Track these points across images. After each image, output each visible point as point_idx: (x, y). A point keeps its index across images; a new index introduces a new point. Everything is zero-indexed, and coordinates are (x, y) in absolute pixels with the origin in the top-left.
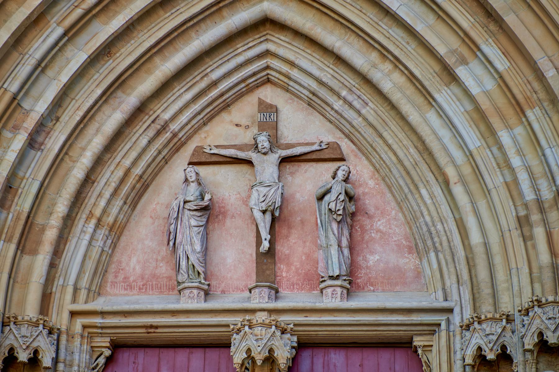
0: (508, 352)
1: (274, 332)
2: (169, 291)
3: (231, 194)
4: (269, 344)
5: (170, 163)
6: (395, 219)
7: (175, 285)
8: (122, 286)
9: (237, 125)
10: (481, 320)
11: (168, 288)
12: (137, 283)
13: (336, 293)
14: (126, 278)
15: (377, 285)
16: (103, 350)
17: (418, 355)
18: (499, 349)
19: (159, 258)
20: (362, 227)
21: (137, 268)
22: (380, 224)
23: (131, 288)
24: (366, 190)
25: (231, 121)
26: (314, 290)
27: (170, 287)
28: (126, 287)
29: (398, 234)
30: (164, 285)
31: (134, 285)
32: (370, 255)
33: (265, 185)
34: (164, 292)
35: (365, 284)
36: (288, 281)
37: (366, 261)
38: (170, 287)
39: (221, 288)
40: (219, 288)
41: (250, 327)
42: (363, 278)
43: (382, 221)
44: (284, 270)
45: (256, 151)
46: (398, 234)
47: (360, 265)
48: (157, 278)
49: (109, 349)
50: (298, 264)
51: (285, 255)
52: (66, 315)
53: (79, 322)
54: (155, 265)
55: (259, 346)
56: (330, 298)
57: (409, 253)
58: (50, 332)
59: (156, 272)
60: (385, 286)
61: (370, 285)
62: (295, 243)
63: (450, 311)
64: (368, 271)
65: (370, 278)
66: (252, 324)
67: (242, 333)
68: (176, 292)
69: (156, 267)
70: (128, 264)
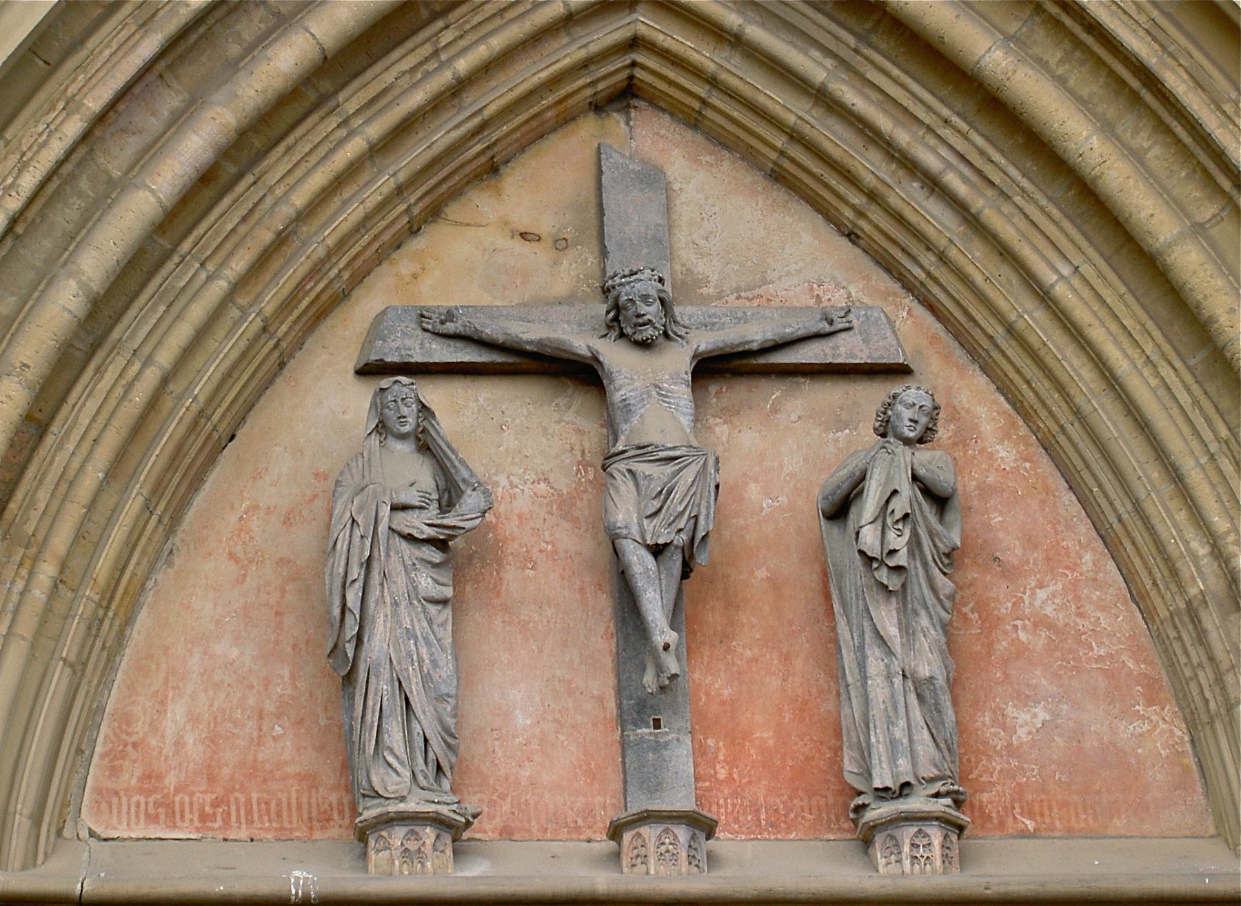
2: (311, 828)
3: (515, 480)
5: (292, 364)
6: (1094, 580)
7: (330, 805)
8: (138, 805)
9: (523, 235)
11: (305, 816)
12: (192, 795)
13: (925, 841)
14: (151, 778)
15: (1046, 812)
19: (270, 707)
20: (983, 607)
21: (190, 739)
23: (171, 814)
25: (505, 223)
26: (830, 830)
27: (314, 814)
28: (151, 811)
29: (1109, 636)
30: (289, 804)
31: (182, 804)
32: (1015, 706)
33: (662, 454)
34: (291, 830)
35: (1005, 808)
36: (735, 794)
38: (314, 814)
39: (498, 820)
40: (491, 817)
42: (999, 788)
43: (1051, 589)
44: (721, 757)
45: (614, 334)
46: (1109, 636)
47: (986, 743)
48: (265, 781)
50: (766, 736)
51: (723, 703)
57: (1150, 702)
59: (260, 756)
60: (1073, 818)
64: (1014, 763)
65: (1020, 788)
68: (338, 830)
69: (260, 737)
70: (154, 728)
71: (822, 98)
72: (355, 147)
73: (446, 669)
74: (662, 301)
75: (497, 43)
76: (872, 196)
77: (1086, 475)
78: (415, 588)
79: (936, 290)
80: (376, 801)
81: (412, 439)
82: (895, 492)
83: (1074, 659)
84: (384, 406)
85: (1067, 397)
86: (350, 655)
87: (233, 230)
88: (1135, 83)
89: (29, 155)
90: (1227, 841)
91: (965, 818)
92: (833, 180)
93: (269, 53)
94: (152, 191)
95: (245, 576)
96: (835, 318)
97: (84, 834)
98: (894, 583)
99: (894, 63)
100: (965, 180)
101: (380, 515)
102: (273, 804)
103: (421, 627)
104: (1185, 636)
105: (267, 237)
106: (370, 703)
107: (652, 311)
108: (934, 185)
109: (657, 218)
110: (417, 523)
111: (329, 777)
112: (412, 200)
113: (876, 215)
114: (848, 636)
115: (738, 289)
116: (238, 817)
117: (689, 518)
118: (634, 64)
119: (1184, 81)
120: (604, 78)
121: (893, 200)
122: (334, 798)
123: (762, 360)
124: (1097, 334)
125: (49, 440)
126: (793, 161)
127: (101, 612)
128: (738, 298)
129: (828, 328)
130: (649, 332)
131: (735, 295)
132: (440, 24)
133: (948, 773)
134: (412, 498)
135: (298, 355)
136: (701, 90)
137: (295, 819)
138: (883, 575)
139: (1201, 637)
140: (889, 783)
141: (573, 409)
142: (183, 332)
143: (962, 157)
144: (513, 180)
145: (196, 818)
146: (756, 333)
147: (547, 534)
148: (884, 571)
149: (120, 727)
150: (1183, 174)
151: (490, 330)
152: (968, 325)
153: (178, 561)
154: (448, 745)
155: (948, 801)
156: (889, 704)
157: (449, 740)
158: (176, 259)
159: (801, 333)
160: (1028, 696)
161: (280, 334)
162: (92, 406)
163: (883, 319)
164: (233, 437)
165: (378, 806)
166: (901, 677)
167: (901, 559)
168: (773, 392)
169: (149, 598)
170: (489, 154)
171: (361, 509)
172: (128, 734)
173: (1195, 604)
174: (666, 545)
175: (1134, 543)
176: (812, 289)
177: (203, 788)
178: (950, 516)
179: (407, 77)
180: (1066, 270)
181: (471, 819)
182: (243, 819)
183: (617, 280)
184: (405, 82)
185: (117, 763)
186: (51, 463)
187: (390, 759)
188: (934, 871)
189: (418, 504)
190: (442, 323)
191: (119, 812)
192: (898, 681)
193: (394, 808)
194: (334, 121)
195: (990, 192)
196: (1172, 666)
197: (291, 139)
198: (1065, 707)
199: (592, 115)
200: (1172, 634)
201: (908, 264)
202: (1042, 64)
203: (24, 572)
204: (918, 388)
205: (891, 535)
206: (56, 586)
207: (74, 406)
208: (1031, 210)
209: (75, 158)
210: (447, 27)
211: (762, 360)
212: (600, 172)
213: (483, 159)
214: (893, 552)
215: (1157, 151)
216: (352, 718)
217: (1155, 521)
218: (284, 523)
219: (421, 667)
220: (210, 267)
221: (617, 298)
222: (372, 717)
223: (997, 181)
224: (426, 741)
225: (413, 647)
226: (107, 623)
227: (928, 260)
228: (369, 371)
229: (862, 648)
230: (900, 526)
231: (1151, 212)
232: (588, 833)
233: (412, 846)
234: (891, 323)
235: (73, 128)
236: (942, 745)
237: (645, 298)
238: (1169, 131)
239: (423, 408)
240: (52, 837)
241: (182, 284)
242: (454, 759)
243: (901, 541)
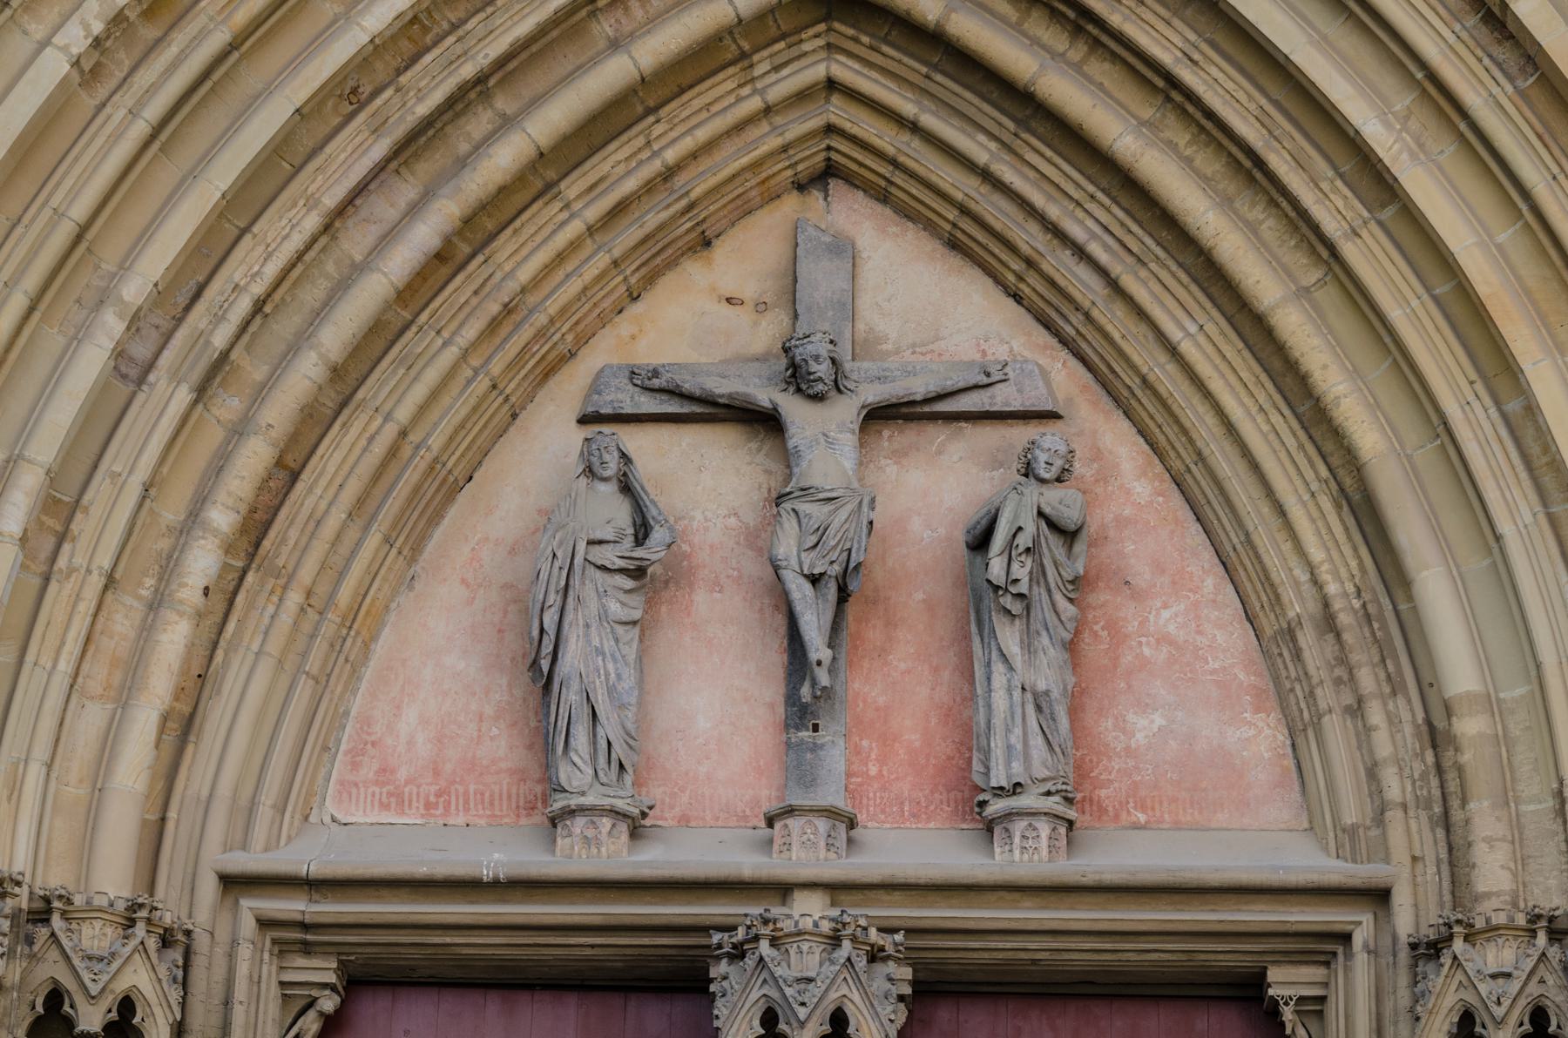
0: (1552, 1029)
1: (849, 959)
2: (518, 816)
4: (833, 995)
5: (523, 415)
6: (1214, 601)
8: (373, 796)
9: (728, 300)
10: (1473, 930)
11: (514, 806)
13: (1035, 834)
15: (1157, 806)
16: (315, 993)
17: (1282, 1025)
18: (1526, 1020)
19: (489, 711)
20: (1112, 626)
22: (1168, 617)
24: (1127, 512)
26: (964, 820)
27: (521, 803)
28: (384, 799)
30: (501, 795)
31: (410, 794)
32: (1135, 713)
33: (821, 496)
35: (1121, 803)
36: (883, 789)
37: (1124, 731)
39: (677, 809)
40: (672, 807)
41: (774, 942)
42: (1116, 785)
43: (1174, 609)
44: (873, 756)
48: (481, 774)
49: (333, 988)
50: (915, 738)
51: (877, 709)
52: (208, 887)
53: (252, 905)
54: (475, 734)
55: (803, 1004)
56: (1017, 852)
57: (1257, 710)
58: (166, 941)
61: (1135, 808)
62: (909, 672)
63: (1379, 897)
64: (1131, 763)
66: (780, 934)
67: (750, 962)
68: (539, 818)
69: (479, 737)
71: (986, 175)
72: (576, 228)
73: (628, 682)
74: (833, 361)
75: (702, 135)
76: (1030, 263)
77: (1206, 507)
78: (606, 611)
79: (1084, 345)
80: (563, 795)
81: (615, 481)
82: (1020, 529)
83: (1191, 671)
84: (590, 454)
85: (1191, 441)
86: (545, 669)
87: (466, 302)
88: (1248, 164)
89: (273, 246)
91: (1072, 814)
92: (997, 249)
93: (491, 151)
94: (385, 274)
95: (474, 598)
96: (992, 370)
97: (327, 819)
98: (1016, 607)
99: (1049, 146)
100: (1106, 247)
101: (577, 548)
102: (487, 795)
103: (609, 645)
104: (1286, 653)
105: (494, 308)
106: (561, 710)
107: (822, 369)
108: (1081, 253)
109: (847, 286)
110: (608, 556)
111: (536, 773)
112: (628, 272)
113: (1033, 278)
114: (981, 653)
115: (914, 345)
116: (457, 805)
117: (842, 551)
118: (829, 148)
119: (1286, 162)
120: (802, 160)
121: (1045, 267)
122: (539, 789)
123: (927, 409)
124: (1216, 385)
125: (300, 487)
126: (963, 231)
127: (344, 631)
128: (914, 353)
129: (986, 380)
130: (820, 387)
131: (911, 350)
132: (651, 119)
133: (1062, 773)
134: (608, 534)
135: (530, 407)
136: (884, 170)
137: (505, 808)
138: (1007, 601)
139: (1297, 655)
140: (1004, 783)
141: (763, 452)
142: (419, 392)
143: (1106, 229)
144: (722, 251)
145: (421, 807)
146: (919, 387)
147: (734, 564)
148: (1009, 597)
149: (361, 728)
150: (1293, 243)
151: (687, 387)
152: (1111, 376)
153: (418, 585)
154: (631, 747)
155: (1057, 798)
156: (1008, 714)
157: (631, 742)
158: (414, 329)
159: (961, 385)
160: (1147, 705)
161: (508, 391)
162: (338, 457)
163: (1037, 371)
164: (471, 478)
165: (564, 799)
166: (1020, 690)
167: (1023, 588)
168: (938, 434)
169: (392, 617)
170: (700, 229)
171: (561, 544)
172: (369, 734)
173: (1293, 624)
174: (821, 575)
175: (1246, 570)
176: (978, 345)
177: (430, 780)
178: (1079, 547)
179: (622, 166)
180: (1193, 329)
181: (647, 811)
182: (461, 808)
183: (793, 342)
184: (621, 169)
185: (358, 759)
186: (302, 505)
187: (576, 759)
188: (1040, 861)
189: (612, 539)
190: (649, 379)
191: (357, 801)
192: (1017, 694)
193: (574, 802)
194: (557, 205)
195: (1130, 260)
196: (1276, 680)
197: (517, 223)
198: (1180, 714)
199: (795, 192)
200: (1276, 651)
201: (1061, 322)
202: (1171, 145)
203: (275, 599)
204: (1053, 435)
205: (1015, 566)
206: (302, 609)
207: (322, 457)
208: (1164, 275)
209: (317, 247)
210: (658, 121)
211: (927, 409)
212: (797, 245)
213: (693, 235)
214: (1016, 581)
215: (1271, 222)
216: (548, 723)
217: (1261, 551)
218: (510, 553)
219: (607, 679)
220: (446, 334)
221: (793, 358)
222: (562, 724)
223: (1135, 249)
224: (609, 743)
225: (601, 663)
226: (349, 640)
227: (1077, 319)
228: (584, 420)
229: (989, 664)
230: (1023, 558)
231: (1257, 278)
232: (755, 822)
233: (590, 833)
234: (1044, 374)
235: (312, 222)
236: (1057, 749)
237: (817, 358)
238: (1277, 205)
239: (623, 455)
240: (296, 823)
241: (420, 350)
242: (636, 758)
243: (1021, 571)
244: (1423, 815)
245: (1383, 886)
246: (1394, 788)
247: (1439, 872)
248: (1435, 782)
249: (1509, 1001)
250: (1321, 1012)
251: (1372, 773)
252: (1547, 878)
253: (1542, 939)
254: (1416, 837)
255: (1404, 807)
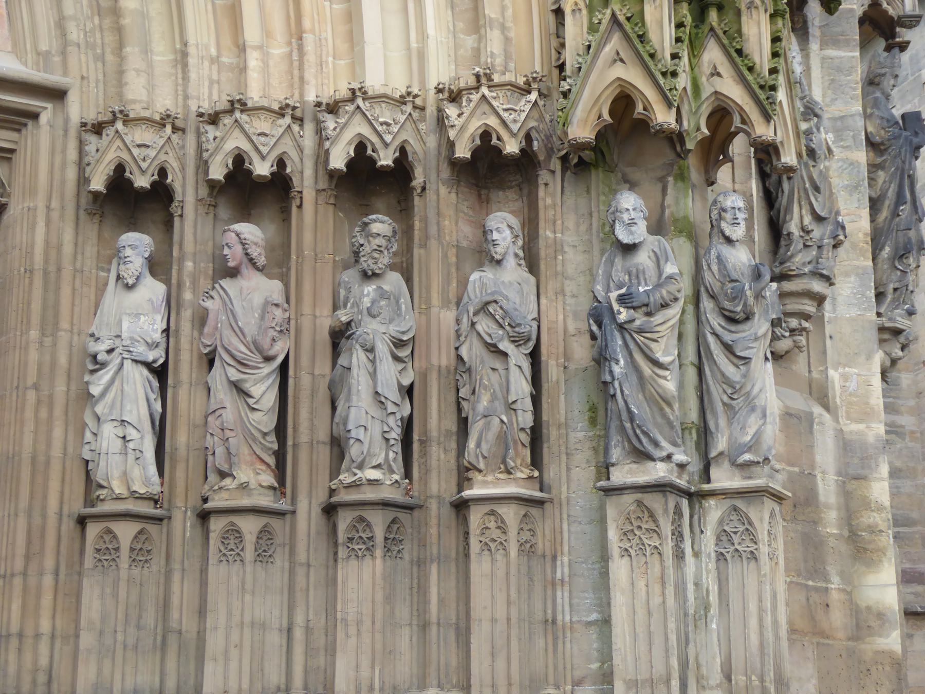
0: (169, 181)
63: (57, 95)
90: (17, 56)
244: (90, 53)
245: (63, 88)
246: (74, 34)
247: (97, 87)
248: (98, 35)
249: (150, 160)
250: (11, 159)
251: (61, 24)
252: (166, 99)
253: (169, 129)
254: (84, 65)
255: (78, 45)
